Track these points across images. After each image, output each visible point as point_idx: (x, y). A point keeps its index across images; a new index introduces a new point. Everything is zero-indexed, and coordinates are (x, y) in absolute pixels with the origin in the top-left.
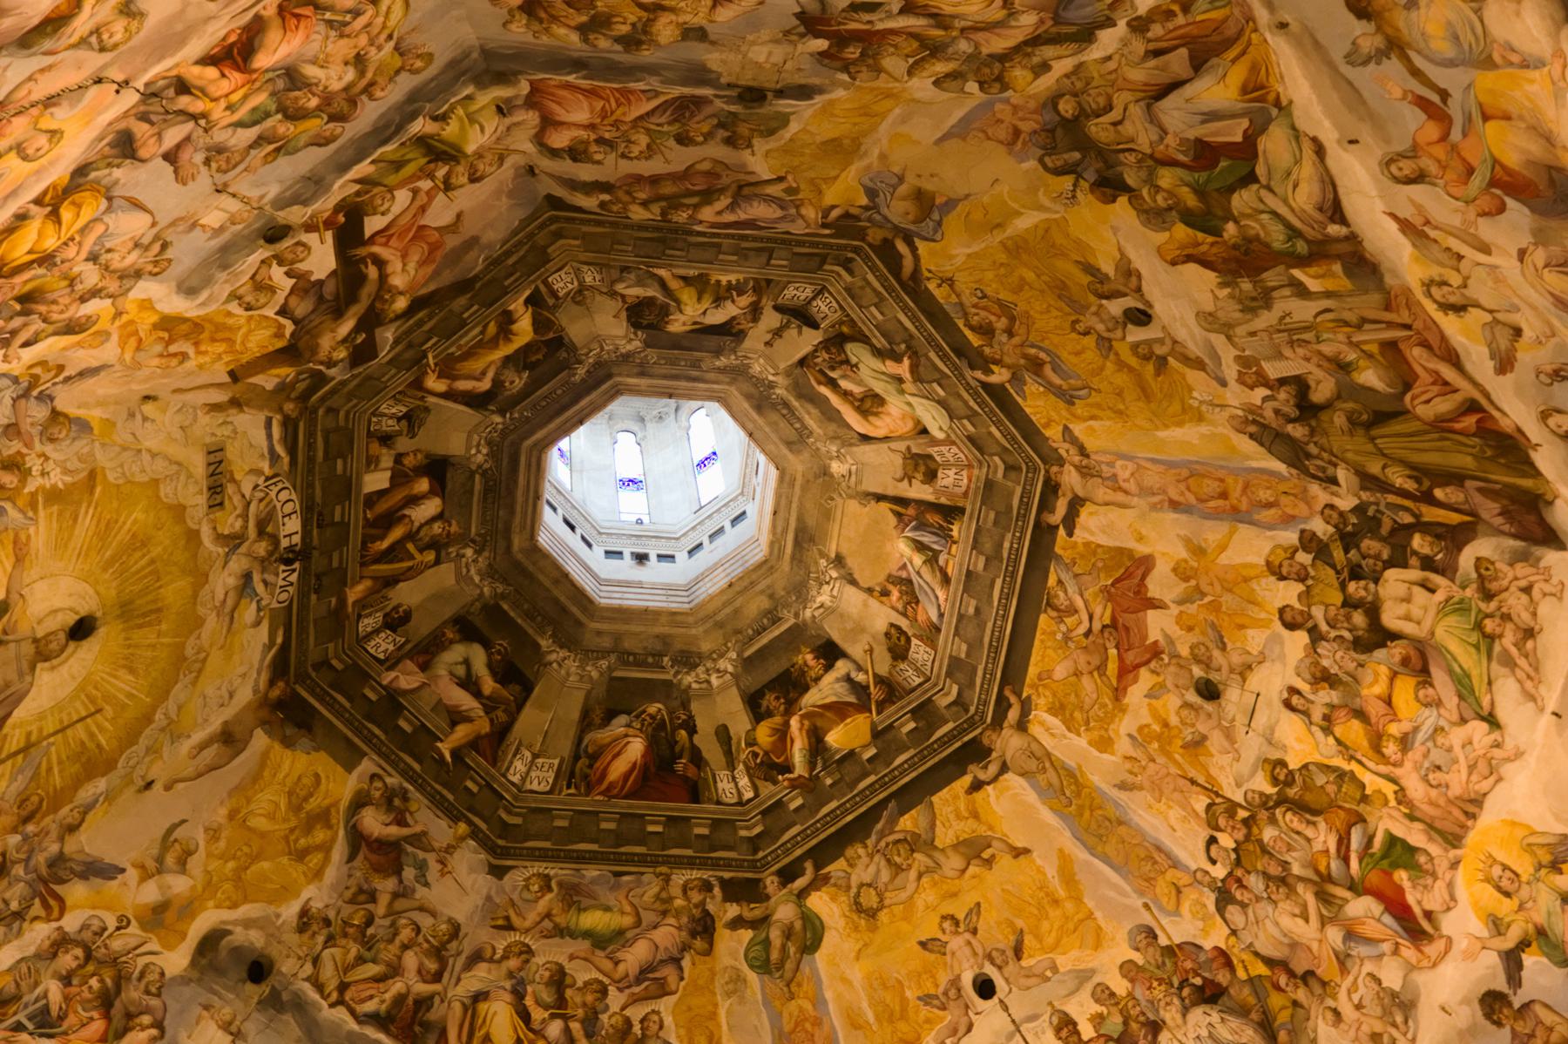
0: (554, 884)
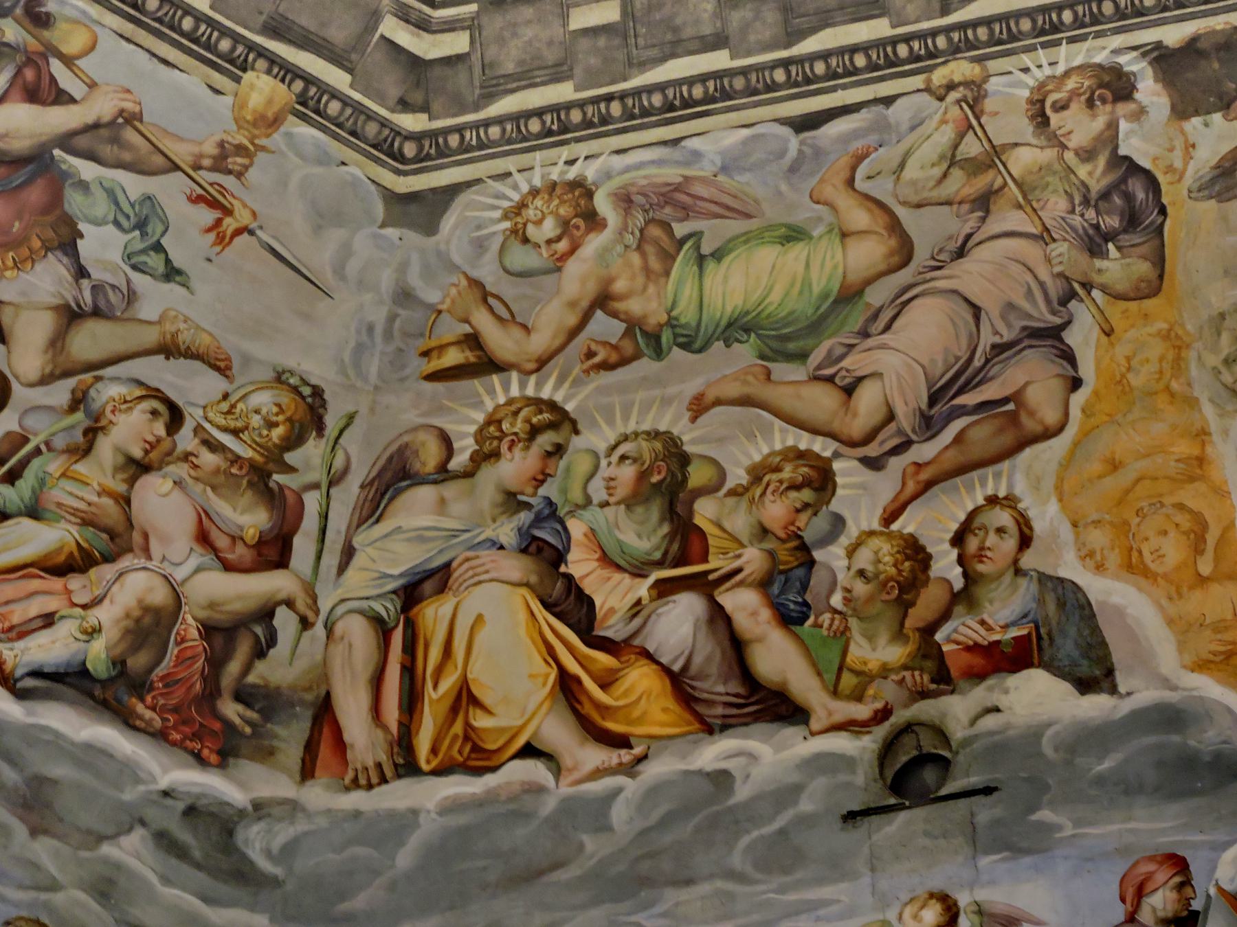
0: (603, 204)
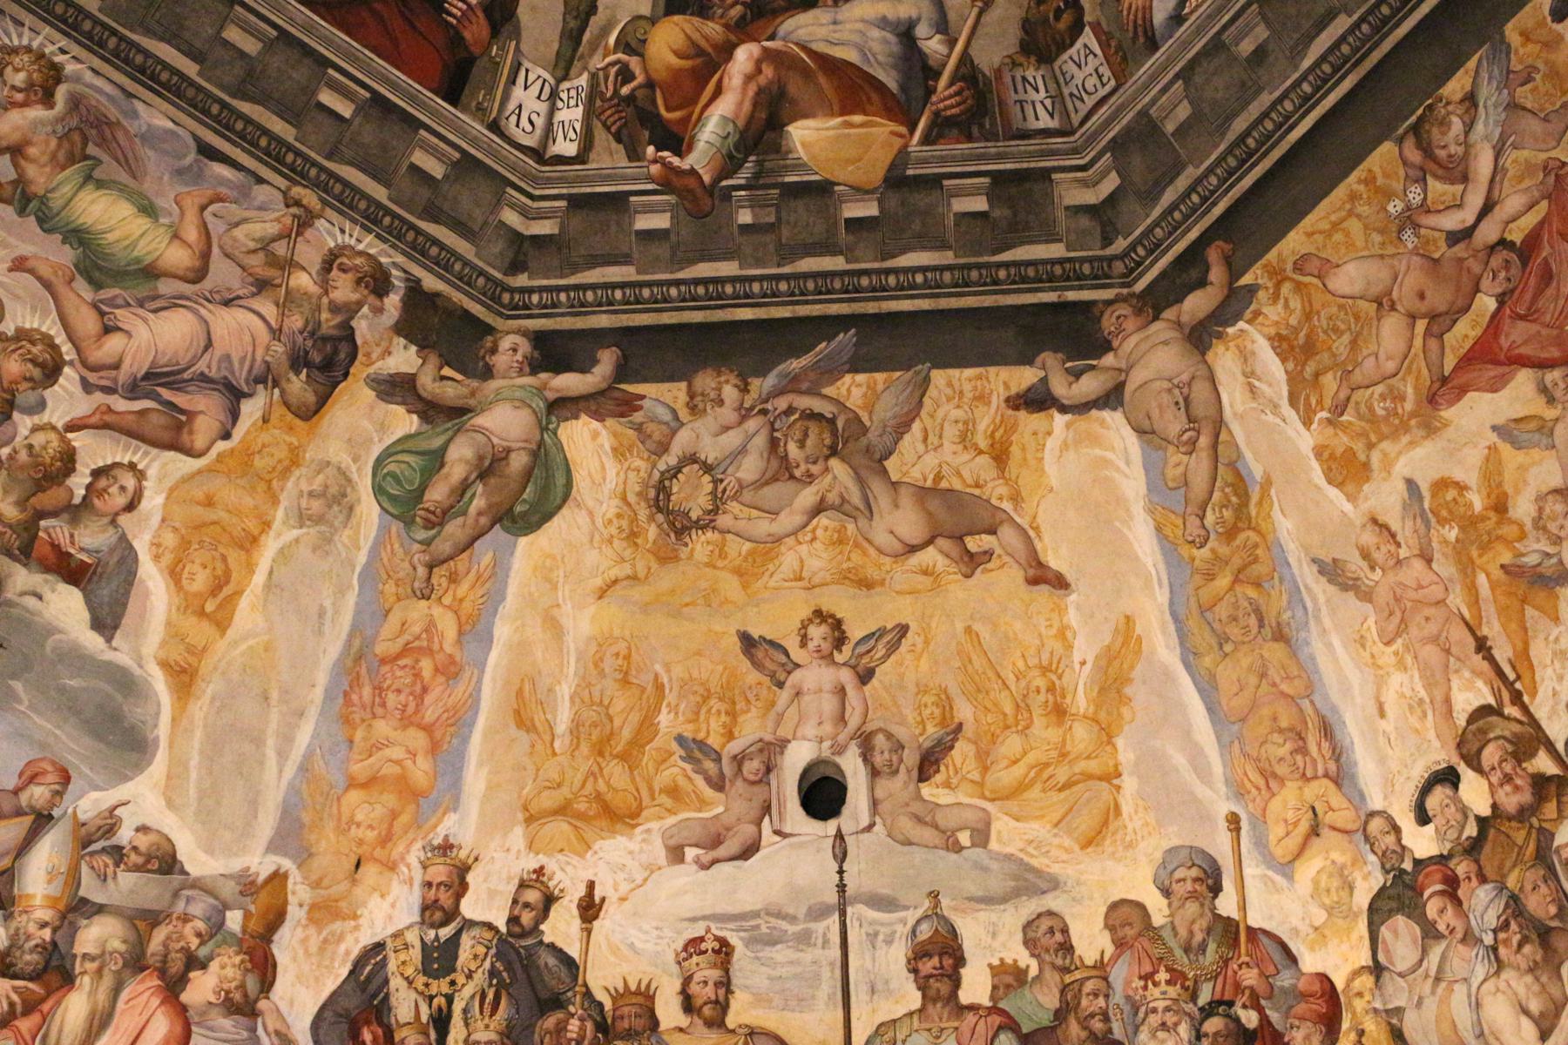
0: (61, 93)
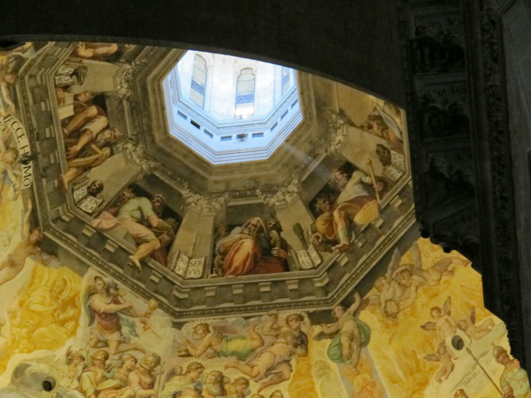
0: (210, 328)
